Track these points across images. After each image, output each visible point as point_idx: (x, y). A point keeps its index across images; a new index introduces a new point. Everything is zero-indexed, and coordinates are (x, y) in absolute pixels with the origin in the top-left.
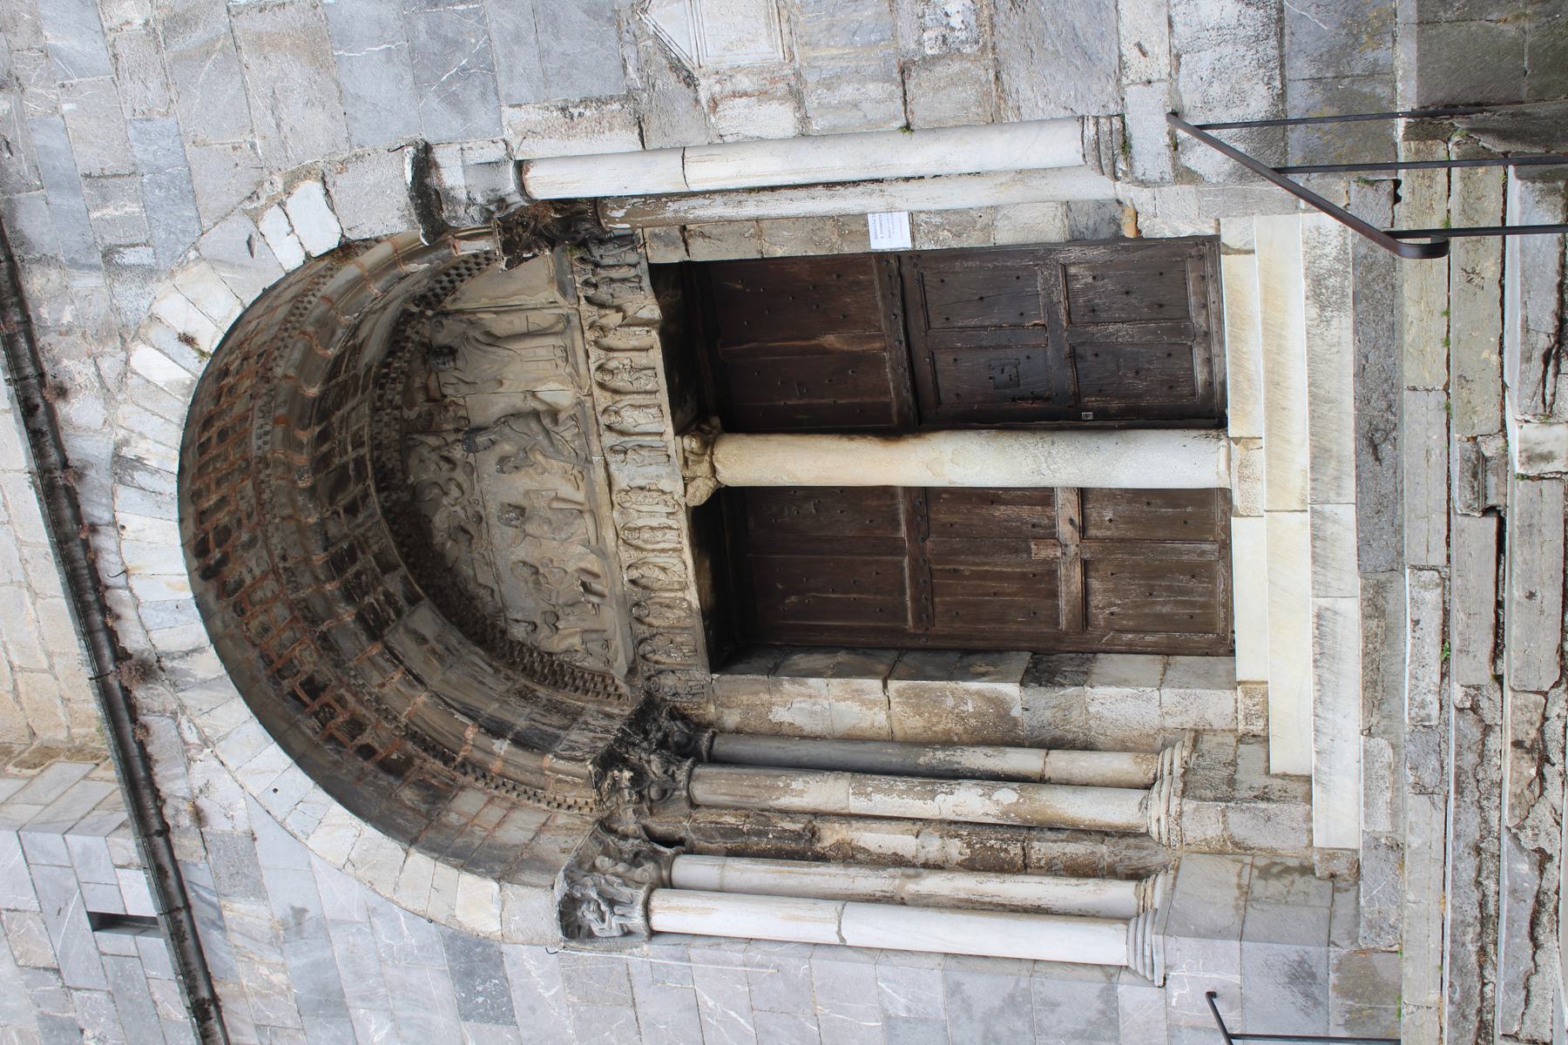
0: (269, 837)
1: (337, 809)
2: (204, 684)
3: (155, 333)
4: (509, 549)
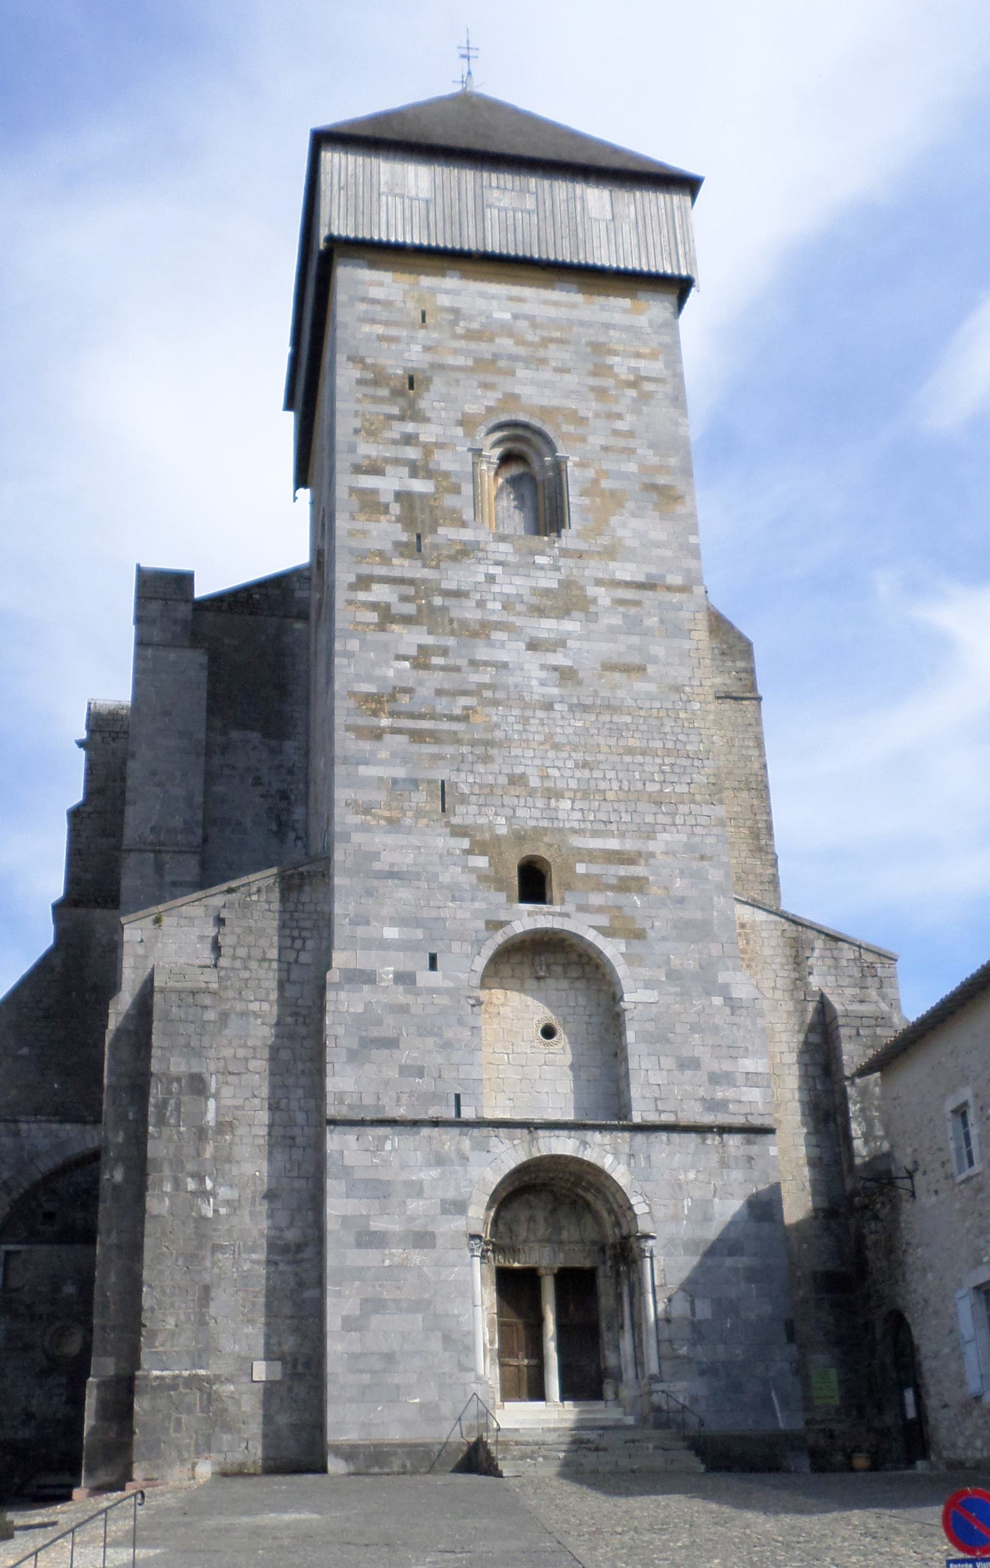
0: (490, 1157)
1: (499, 1179)
2: (530, 1150)
3: (616, 1162)
4: (524, 1215)
